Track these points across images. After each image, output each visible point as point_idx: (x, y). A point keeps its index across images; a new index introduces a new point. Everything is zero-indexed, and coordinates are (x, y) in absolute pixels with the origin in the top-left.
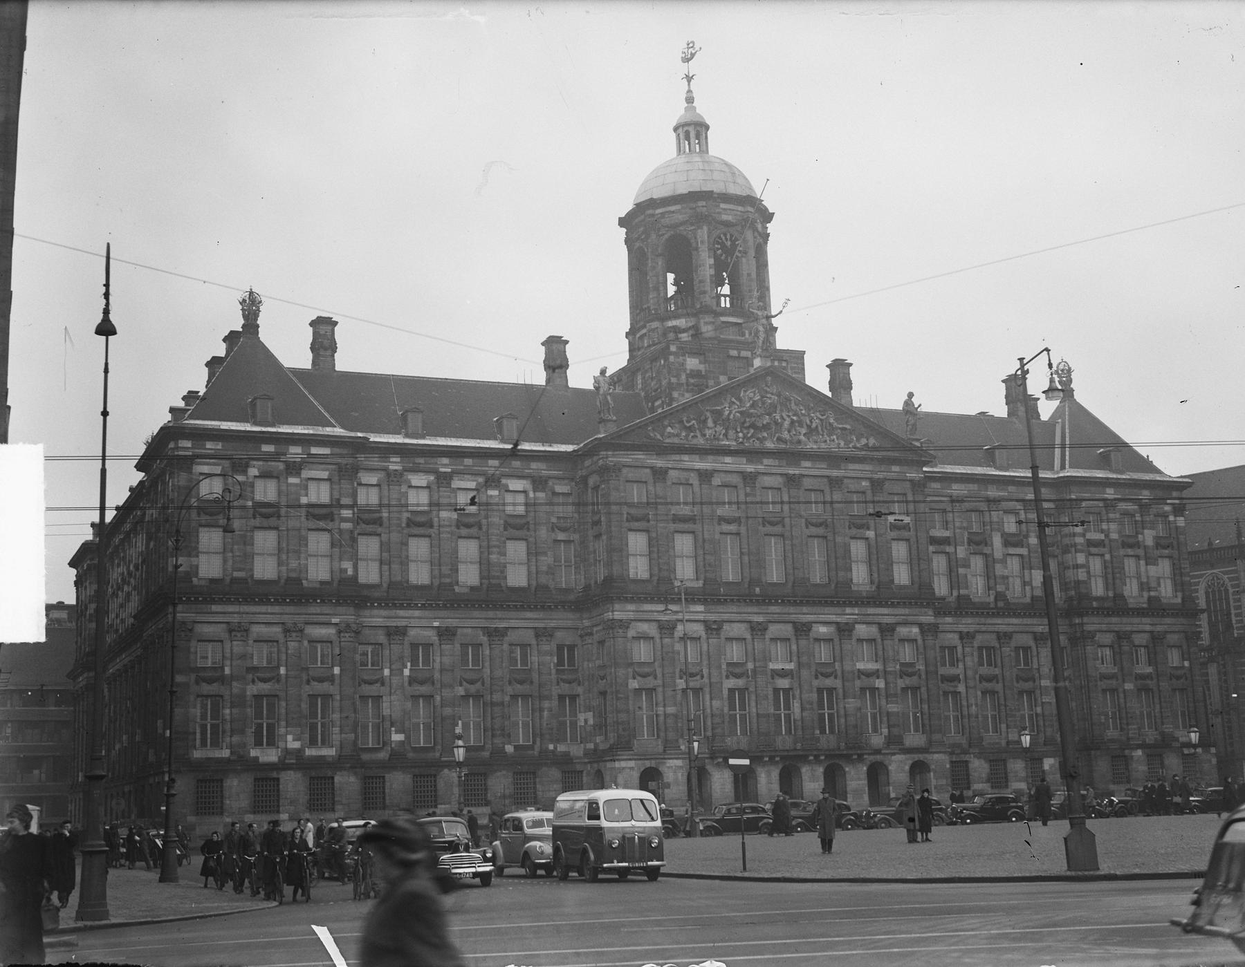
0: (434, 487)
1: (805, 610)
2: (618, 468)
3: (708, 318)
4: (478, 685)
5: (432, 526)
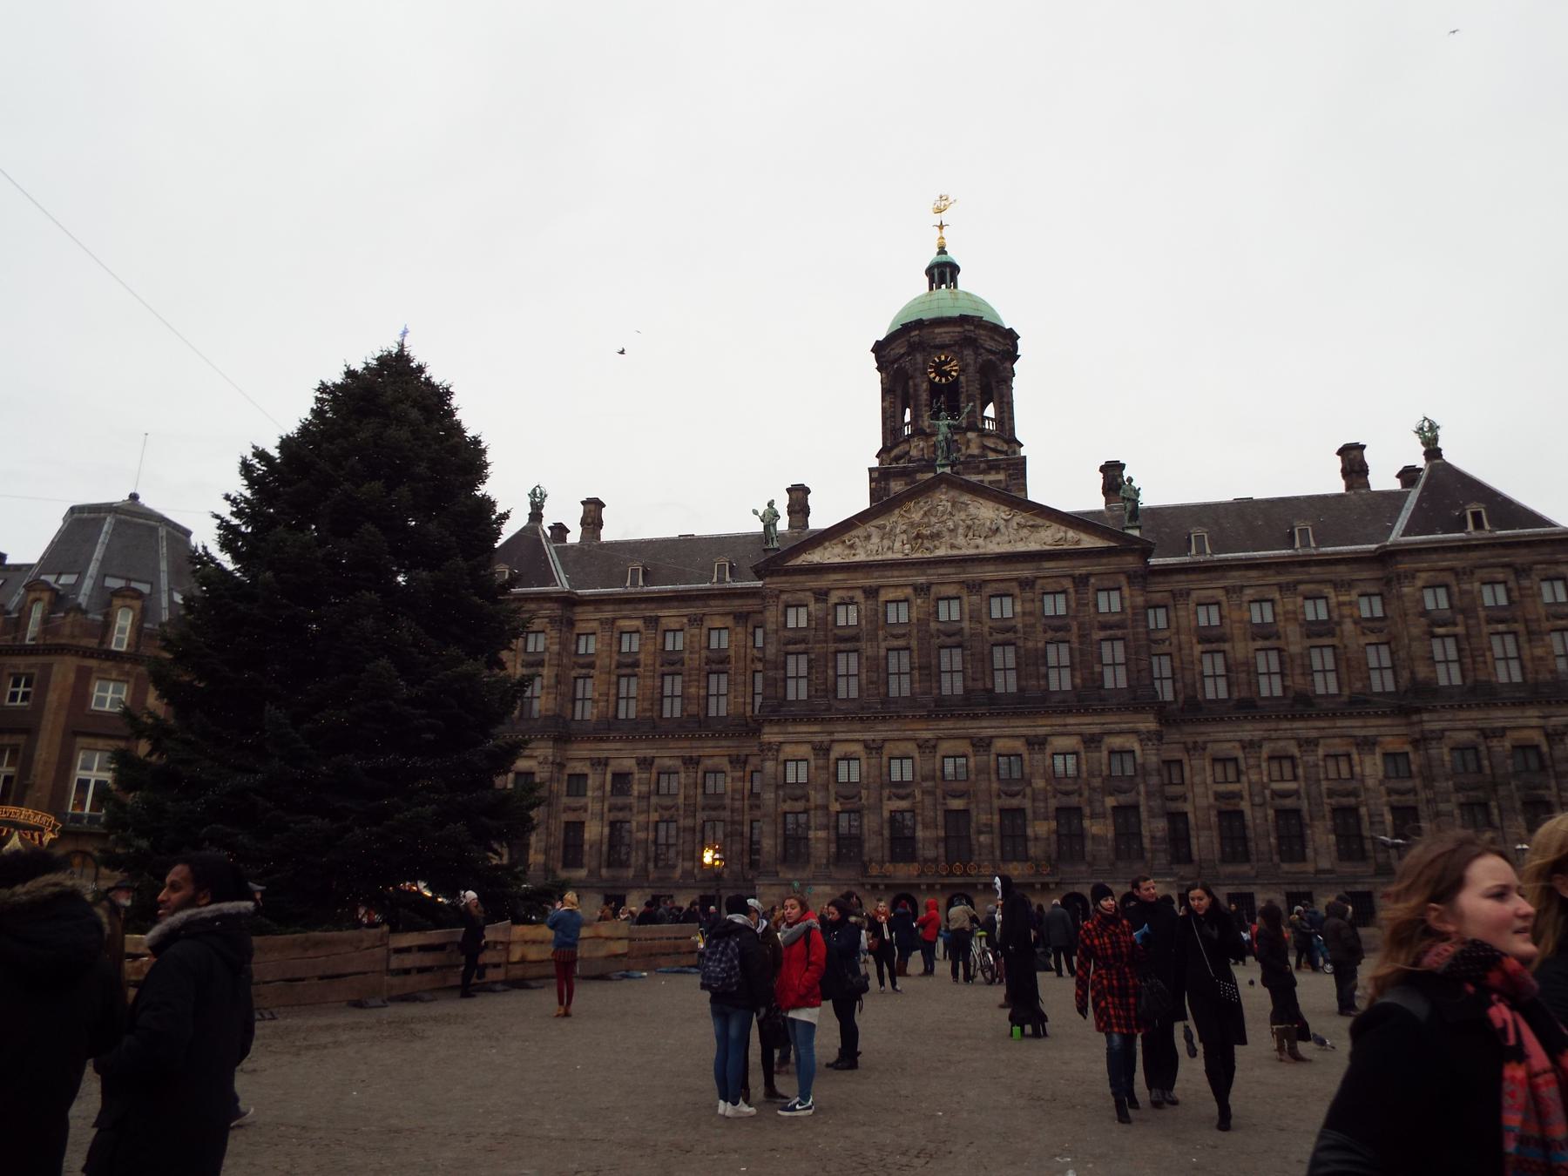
0: (642, 628)
1: (984, 723)
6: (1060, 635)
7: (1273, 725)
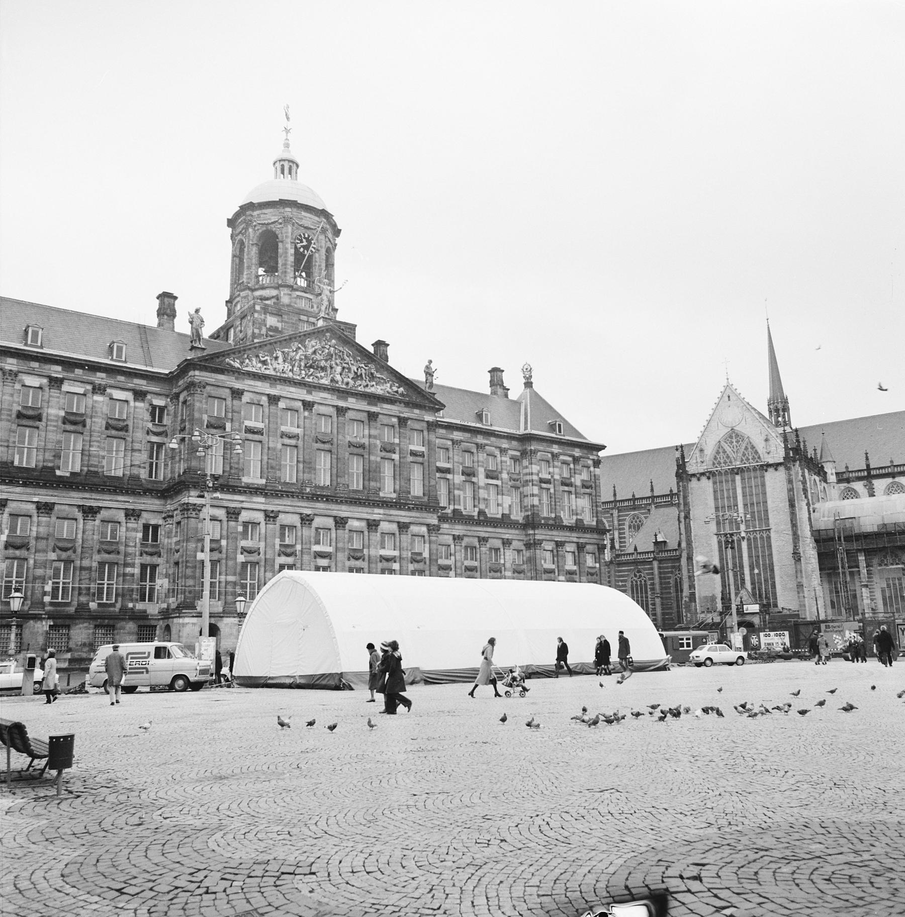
0: (47, 389)
1: (344, 507)
2: (205, 385)
3: (286, 291)
4: (70, 553)
5: (40, 420)
6: (388, 455)
7: (469, 528)
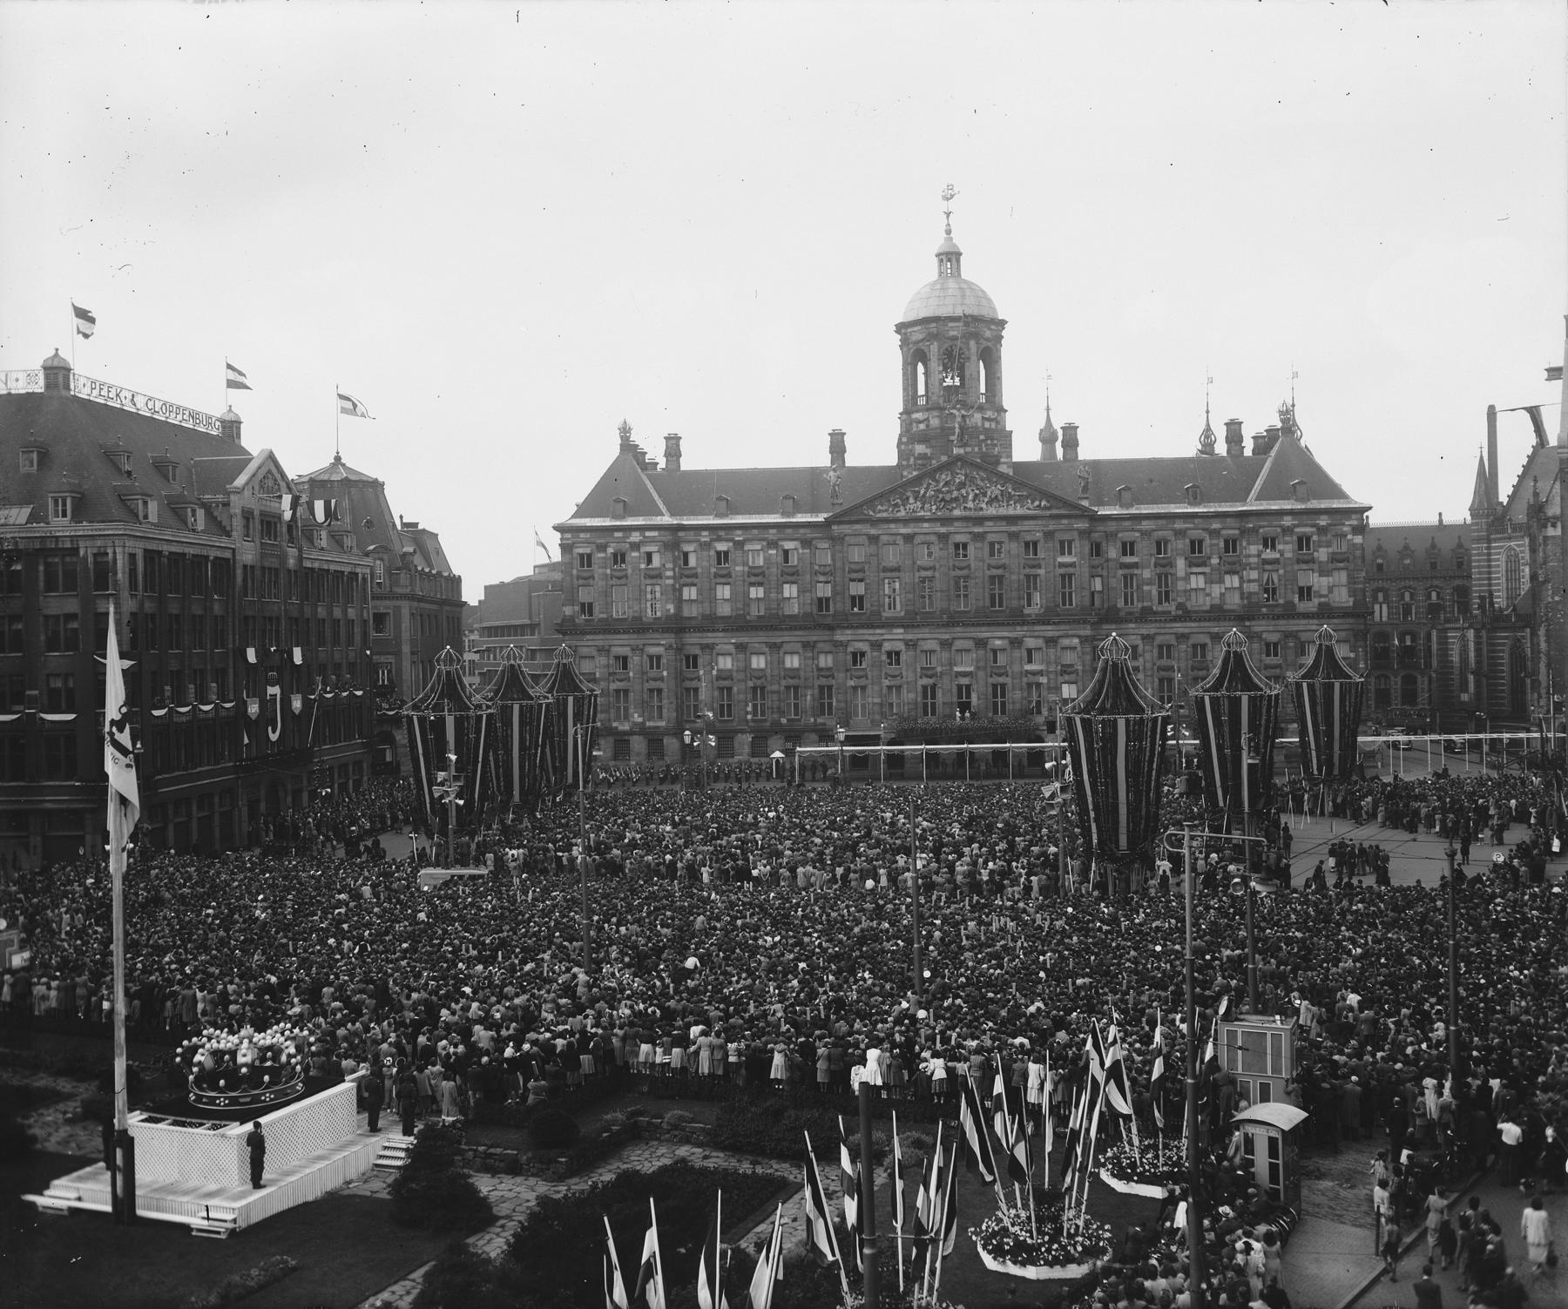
3: (936, 413)
